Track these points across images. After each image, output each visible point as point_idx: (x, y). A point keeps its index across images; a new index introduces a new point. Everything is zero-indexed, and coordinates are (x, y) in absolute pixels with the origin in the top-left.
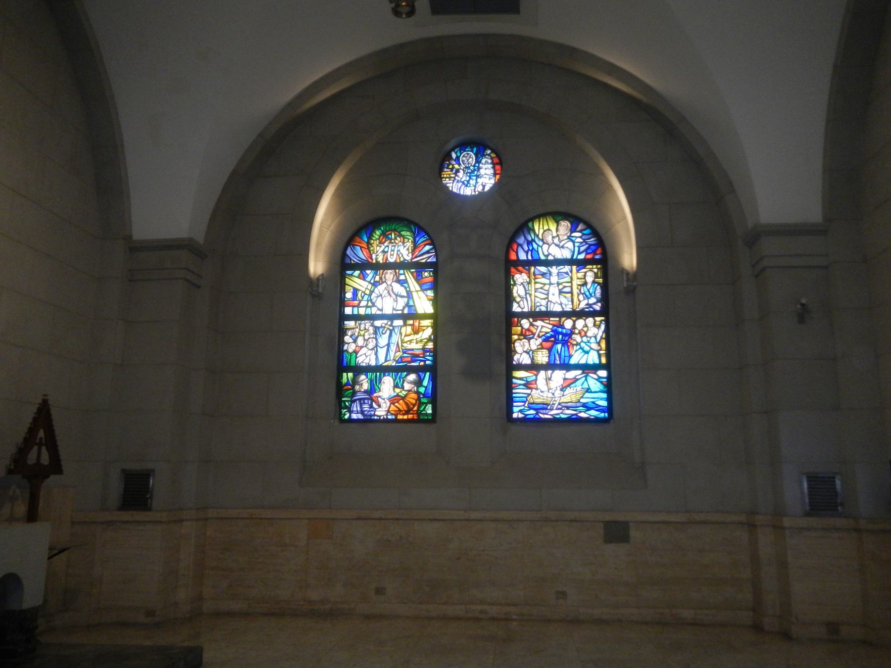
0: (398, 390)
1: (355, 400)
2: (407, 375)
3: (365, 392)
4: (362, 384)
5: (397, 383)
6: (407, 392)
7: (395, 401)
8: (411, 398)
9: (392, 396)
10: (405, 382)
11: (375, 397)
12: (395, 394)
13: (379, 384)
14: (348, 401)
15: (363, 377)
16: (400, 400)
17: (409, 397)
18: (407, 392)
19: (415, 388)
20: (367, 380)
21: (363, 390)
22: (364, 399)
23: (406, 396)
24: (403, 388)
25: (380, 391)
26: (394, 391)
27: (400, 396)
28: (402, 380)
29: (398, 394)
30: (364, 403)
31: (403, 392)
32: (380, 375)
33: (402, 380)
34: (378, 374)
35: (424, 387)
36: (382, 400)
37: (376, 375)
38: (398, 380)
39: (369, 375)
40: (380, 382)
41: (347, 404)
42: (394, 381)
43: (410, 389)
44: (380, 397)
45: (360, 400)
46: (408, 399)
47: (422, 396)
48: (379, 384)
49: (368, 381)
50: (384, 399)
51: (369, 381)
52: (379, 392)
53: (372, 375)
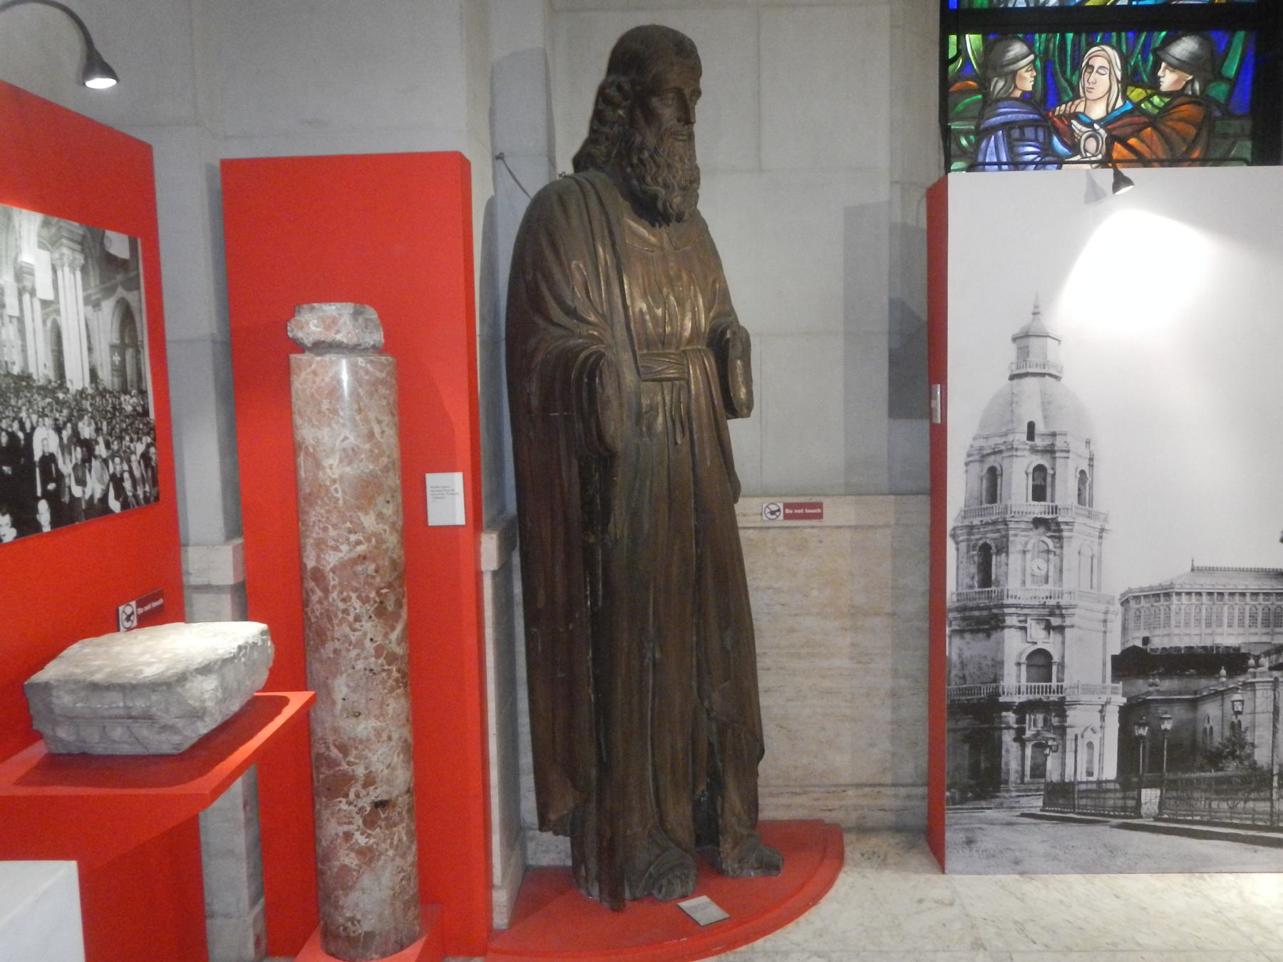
0: (1136, 94)
1: (993, 130)
2: (1168, 42)
3: (1026, 98)
4: (1014, 73)
5: (1135, 68)
6: (1167, 100)
7: (1129, 130)
8: (1181, 120)
9: (1117, 113)
10: (1163, 65)
11: (1059, 117)
12: (1129, 106)
13: (1073, 73)
14: (966, 134)
15: (1018, 48)
16: (1145, 126)
17: (1175, 116)
18: (1167, 100)
19: (1197, 86)
20: (1032, 57)
21: (1018, 94)
22: (1022, 125)
23: (1165, 110)
24: (1154, 84)
25: (1077, 96)
26: (1125, 98)
27: (1144, 113)
28: (1151, 58)
29: (1137, 106)
30: (1023, 139)
31: (1156, 100)
32: (1076, 44)
33: (1151, 58)
34: (1070, 36)
35: (1228, 80)
36: (1084, 129)
37: (1063, 39)
38: (1136, 58)
39: (1040, 39)
40: (1076, 66)
41: (964, 142)
42: (1125, 59)
43: (1179, 87)
44: (1076, 116)
45: (1006, 127)
46: (1170, 123)
47: (1217, 113)
48: (1073, 73)
49: (1033, 62)
50: (1090, 124)
51: (1038, 63)
52: (1073, 100)
53: (1048, 41)
